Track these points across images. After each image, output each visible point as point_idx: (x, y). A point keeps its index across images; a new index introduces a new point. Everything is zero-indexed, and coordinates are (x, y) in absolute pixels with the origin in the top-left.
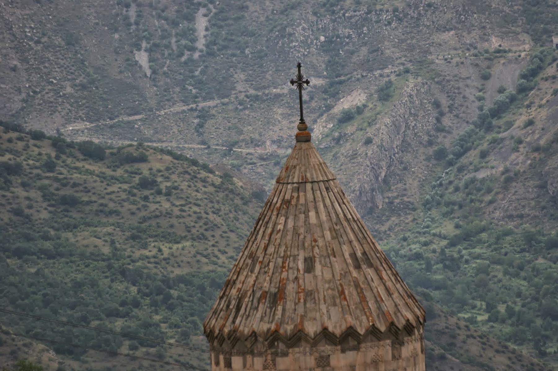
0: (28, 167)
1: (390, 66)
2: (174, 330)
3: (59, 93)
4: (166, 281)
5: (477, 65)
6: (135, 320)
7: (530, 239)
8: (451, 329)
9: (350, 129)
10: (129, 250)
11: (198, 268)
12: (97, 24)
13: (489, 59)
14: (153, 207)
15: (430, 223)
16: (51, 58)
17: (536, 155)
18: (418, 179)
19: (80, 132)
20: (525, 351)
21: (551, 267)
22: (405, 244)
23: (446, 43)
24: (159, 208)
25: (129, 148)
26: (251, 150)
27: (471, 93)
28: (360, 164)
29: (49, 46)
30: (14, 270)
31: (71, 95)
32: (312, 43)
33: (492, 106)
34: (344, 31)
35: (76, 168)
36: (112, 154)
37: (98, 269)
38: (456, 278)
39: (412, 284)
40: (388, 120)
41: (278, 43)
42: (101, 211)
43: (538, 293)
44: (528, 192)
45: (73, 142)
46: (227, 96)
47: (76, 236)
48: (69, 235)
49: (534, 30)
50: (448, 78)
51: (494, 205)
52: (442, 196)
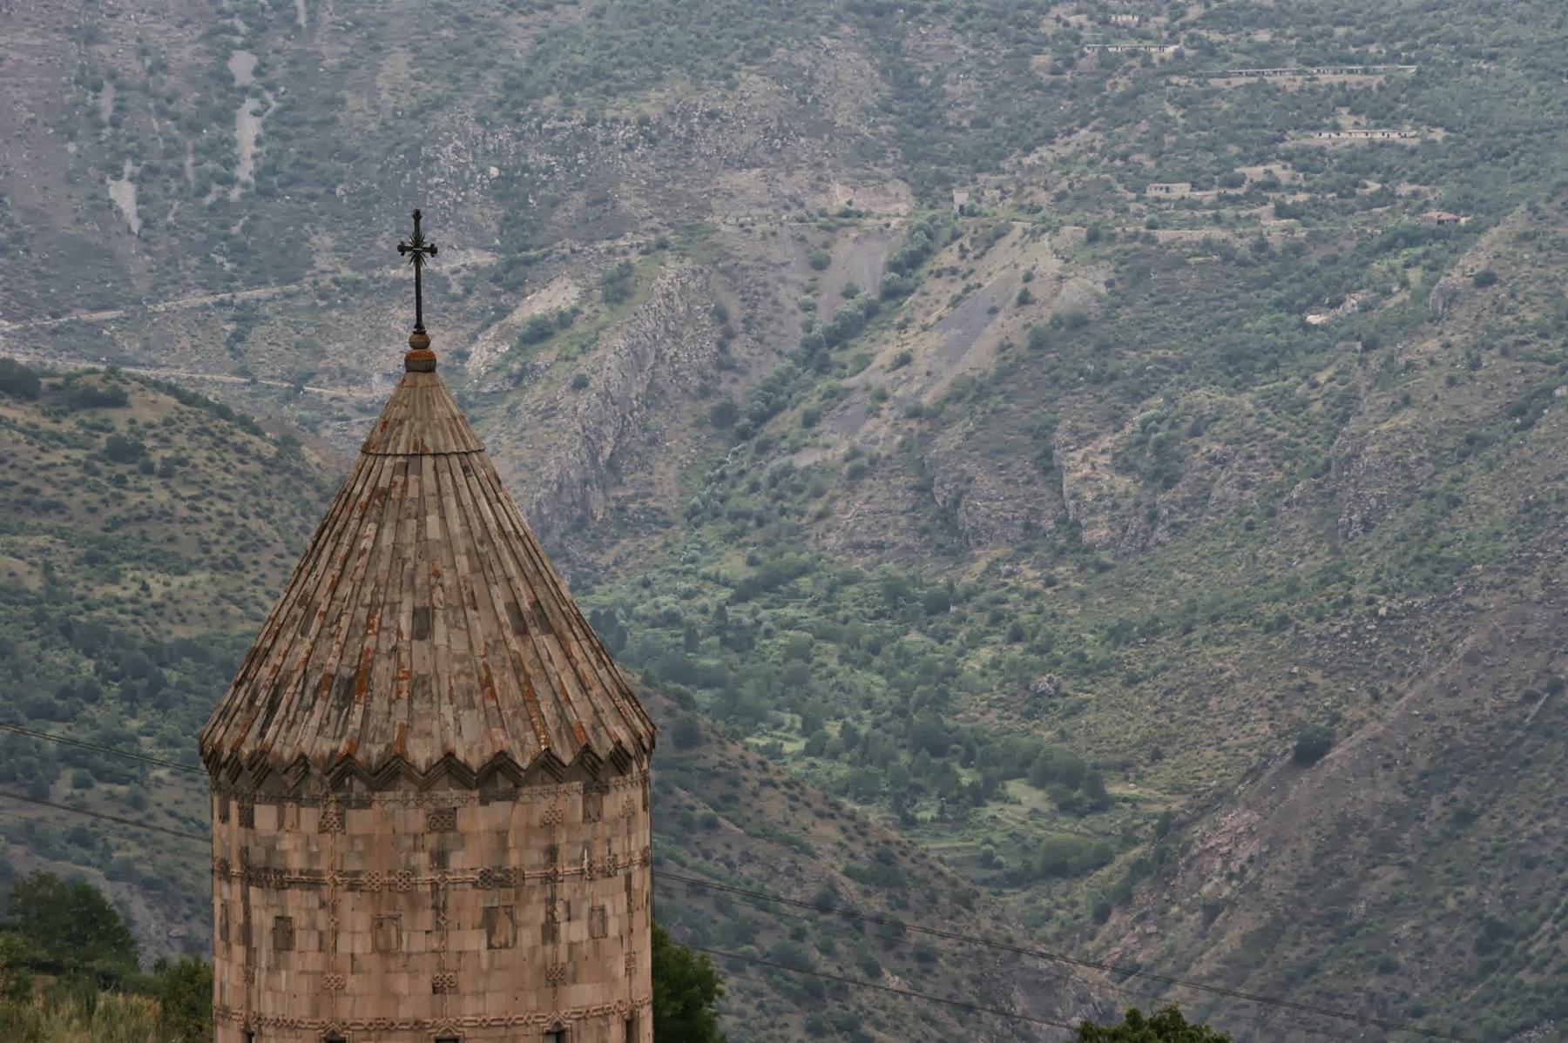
1: (629, 234)
5: (803, 239)
6: (87, 727)
7: (894, 592)
9: (544, 356)
10: (81, 584)
11: (225, 627)
12: (32, 121)
13: (829, 229)
14: (133, 499)
17: (913, 424)
18: (676, 464)
20: (874, 814)
21: (933, 650)
22: (647, 593)
23: (742, 192)
25: (87, 378)
26: (341, 392)
27: (789, 296)
28: (560, 429)
32: (472, 179)
33: (831, 324)
34: (537, 158)
36: (54, 387)
37: (16, 621)
38: (747, 664)
40: (620, 343)
41: (403, 176)
42: (27, 503)
43: (906, 700)
44: (895, 498)
46: (295, 280)
49: (916, 175)
50: (743, 262)
51: (828, 521)
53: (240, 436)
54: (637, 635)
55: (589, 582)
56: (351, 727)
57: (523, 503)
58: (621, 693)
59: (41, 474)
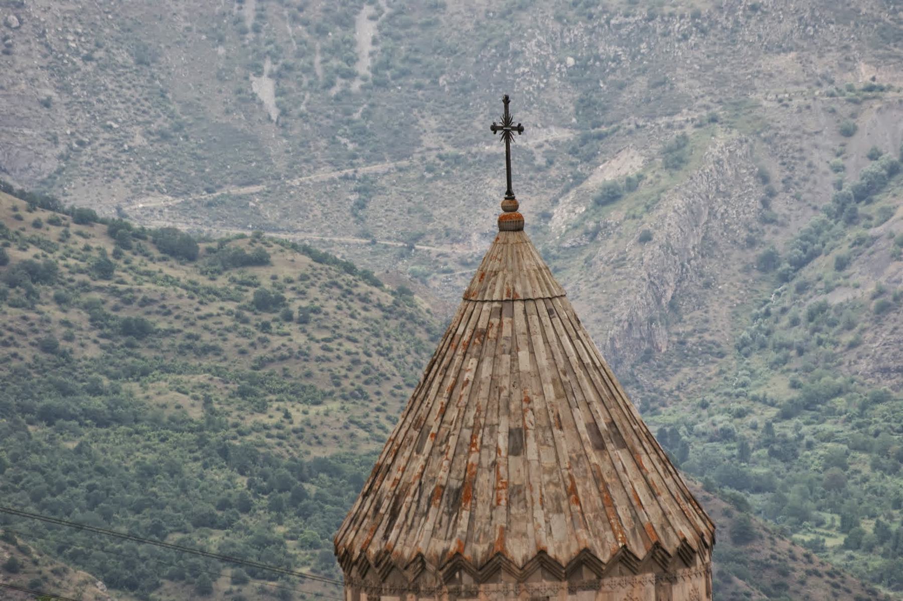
0: (67, 270)
1: (685, 111)
2: (309, 552)
3: (122, 145)
4: (296, 468)
5: (833, 111)
6: (242, 532)
8: (780, 560)
9: (614, 215)
11: (352, 447)
12: (189, 29)
14: (276, 342)
15: (748, 379)
16: (110, 86)
18: (728, 304)
19: (155, 213)
22: (705, 413)
23: (781, 72)
24: (288, 343)
27: (822, 159)
29: (106, 66)
30: (40, 445)
31: (143, 149)
32: (552, 68)
33: (858, 182)
34: (608, 49)
35: (148, 274)
36: (210, 250)
37: (182, 445)
38: (791, 472)
39: (714, 481)
40: (678, 203)
41: (495, 67)
42: (189, 347)
45: (143, 229)
46: (408, 156)
47: (146, 389)
48: (135, 386)
50: (783, 132)
51: (858, 349)
52: (768, 333)
53: (363, 288)
54: (698, 449)
55: (656, 404)
56: (459, 530)
57: (599, 338)
58: (685, 497)
59: (200, 323)
